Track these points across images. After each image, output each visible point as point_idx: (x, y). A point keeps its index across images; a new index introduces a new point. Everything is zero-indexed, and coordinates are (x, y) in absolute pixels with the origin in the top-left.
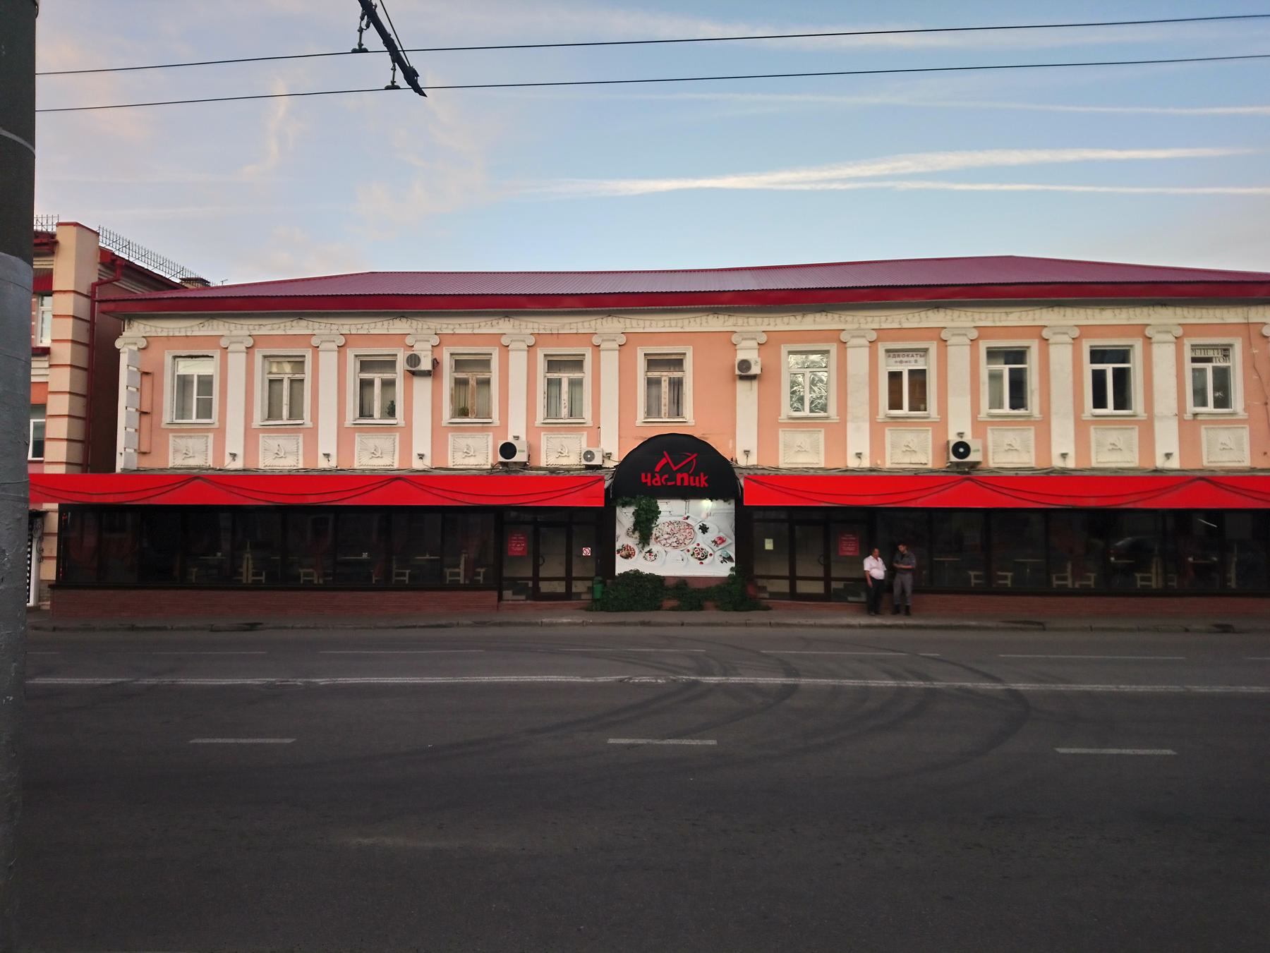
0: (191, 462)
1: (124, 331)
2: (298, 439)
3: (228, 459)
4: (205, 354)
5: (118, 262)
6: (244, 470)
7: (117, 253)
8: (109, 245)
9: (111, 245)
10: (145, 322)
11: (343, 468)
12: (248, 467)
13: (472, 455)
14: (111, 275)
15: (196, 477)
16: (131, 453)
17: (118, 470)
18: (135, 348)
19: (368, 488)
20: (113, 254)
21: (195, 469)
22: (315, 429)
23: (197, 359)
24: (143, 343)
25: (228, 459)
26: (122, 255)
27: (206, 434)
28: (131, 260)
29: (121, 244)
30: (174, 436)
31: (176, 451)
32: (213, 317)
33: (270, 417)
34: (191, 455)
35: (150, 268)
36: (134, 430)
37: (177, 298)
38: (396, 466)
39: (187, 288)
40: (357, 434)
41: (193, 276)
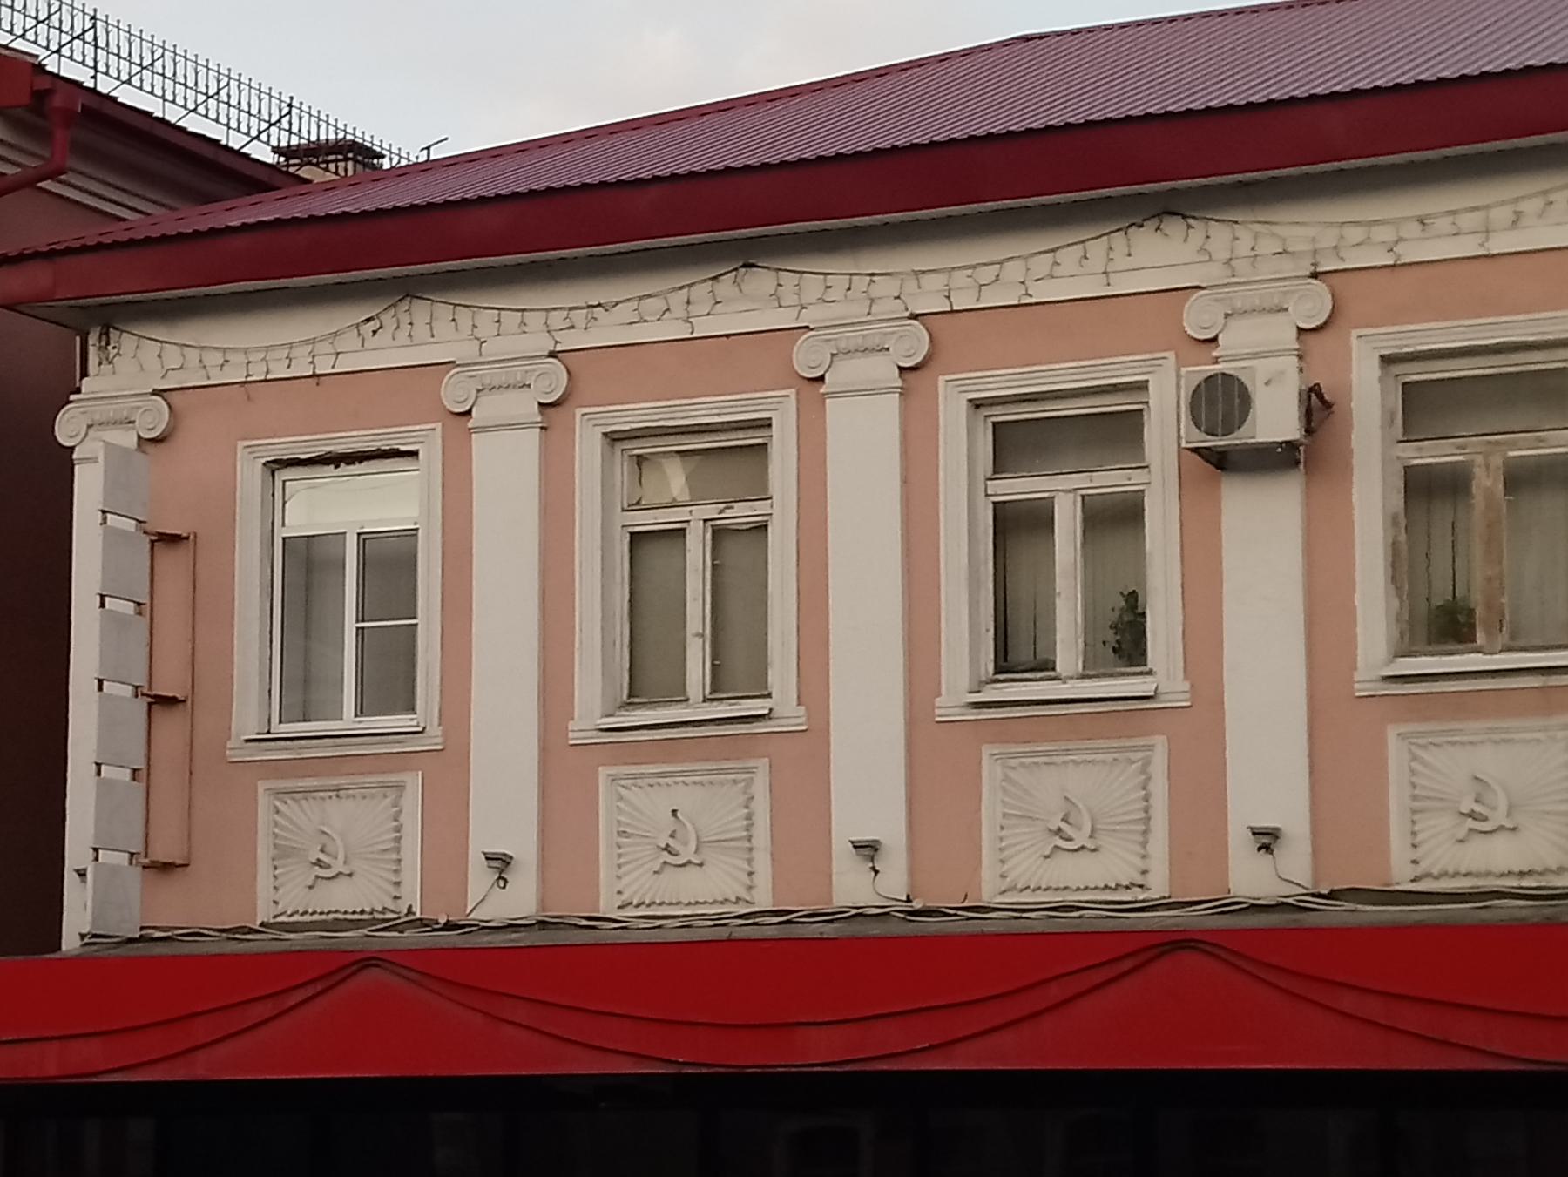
0: (343, 899)
1: (84, 374)
2: (750, 782)
3: (479, 877)
4: (384, 445)
5: (57, 101)
6: (543, 925)
7: (52, 65)
8: (23, 36)
9: (30, 35)
10: (159, 332)
11: (932, 904)
12: (554, 911)
13: (1501, 828)
14: (33, 155)
15: (368, 961)
16: (114, 870)
17: (70, 942)
18: (128, 439)
19: (1055, 992)
20: (40, 68)
21: (357, 924)
22: (816, 736)
23: (356, 468)
24: (155, 418)
25: (479, 877)
26: (70, 71)
27: (393, 778)
28: (104, 86)
29: (66, 28)
30: (278, 793)
31: (282, 853)
32: (409, 290)
33: (637, 691)
34: (338, 866)
35: (172, 115)
36: (127, 774)
37: (278, 222)
38: (1158, 888)
39: (307, 181)
40: (987, 750)
41: (327, 134)
